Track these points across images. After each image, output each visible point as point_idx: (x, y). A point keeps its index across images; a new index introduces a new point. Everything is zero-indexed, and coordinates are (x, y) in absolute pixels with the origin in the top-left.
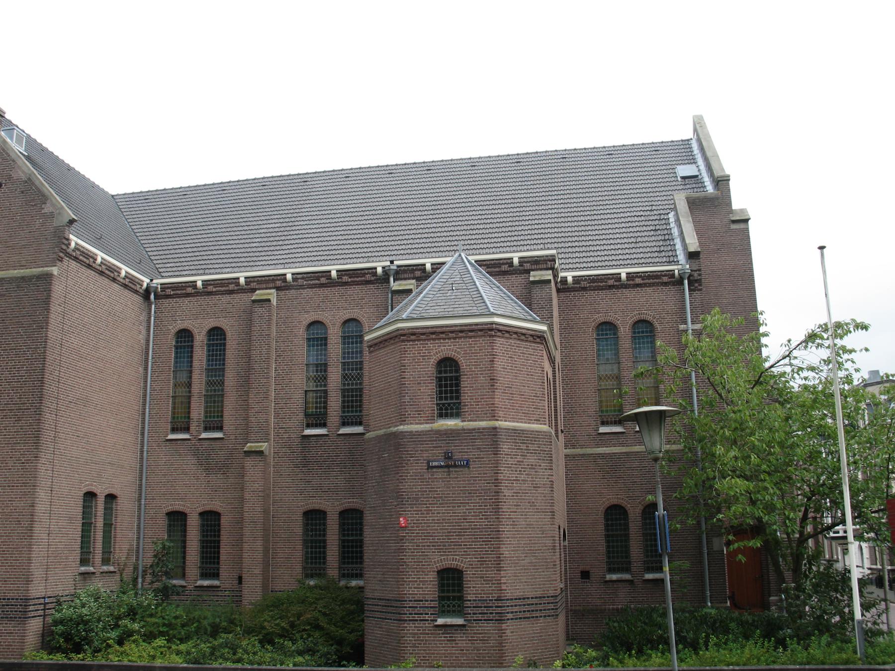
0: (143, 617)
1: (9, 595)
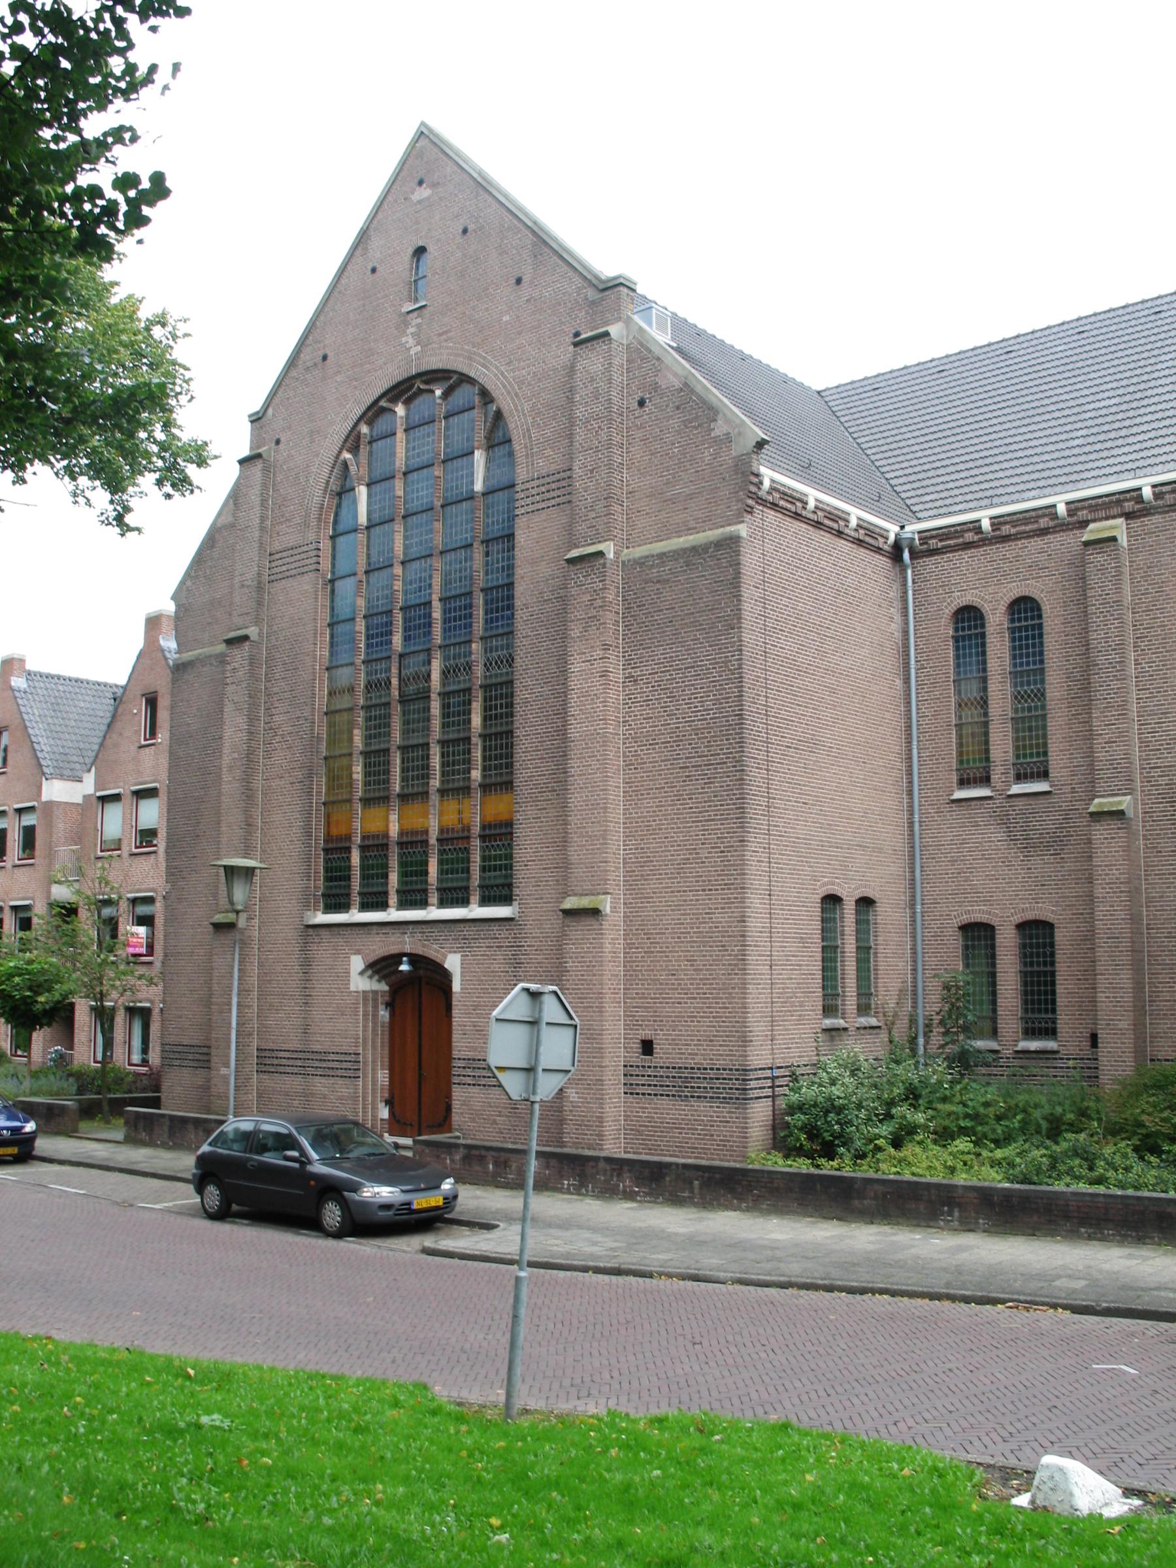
0: (930, 1102)
1: (719, 1063)
